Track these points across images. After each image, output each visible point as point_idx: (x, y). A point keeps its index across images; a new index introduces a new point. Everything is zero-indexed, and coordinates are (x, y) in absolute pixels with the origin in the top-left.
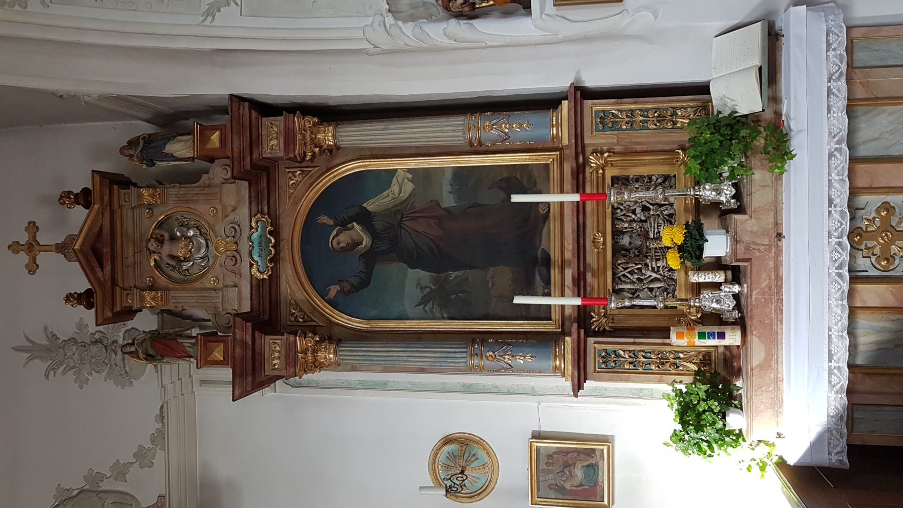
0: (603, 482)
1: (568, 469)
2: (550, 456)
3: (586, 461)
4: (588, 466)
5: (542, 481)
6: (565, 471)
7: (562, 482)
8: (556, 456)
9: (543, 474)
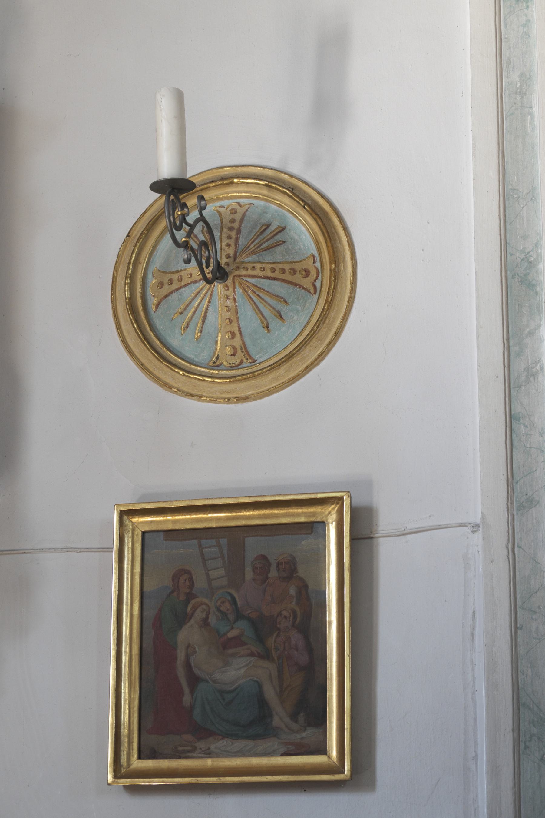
0: (209, 754)
5: (200, 545)
6: (243, 625)
7: (199, 615)
8: (292, 591)
9: (225, 549)
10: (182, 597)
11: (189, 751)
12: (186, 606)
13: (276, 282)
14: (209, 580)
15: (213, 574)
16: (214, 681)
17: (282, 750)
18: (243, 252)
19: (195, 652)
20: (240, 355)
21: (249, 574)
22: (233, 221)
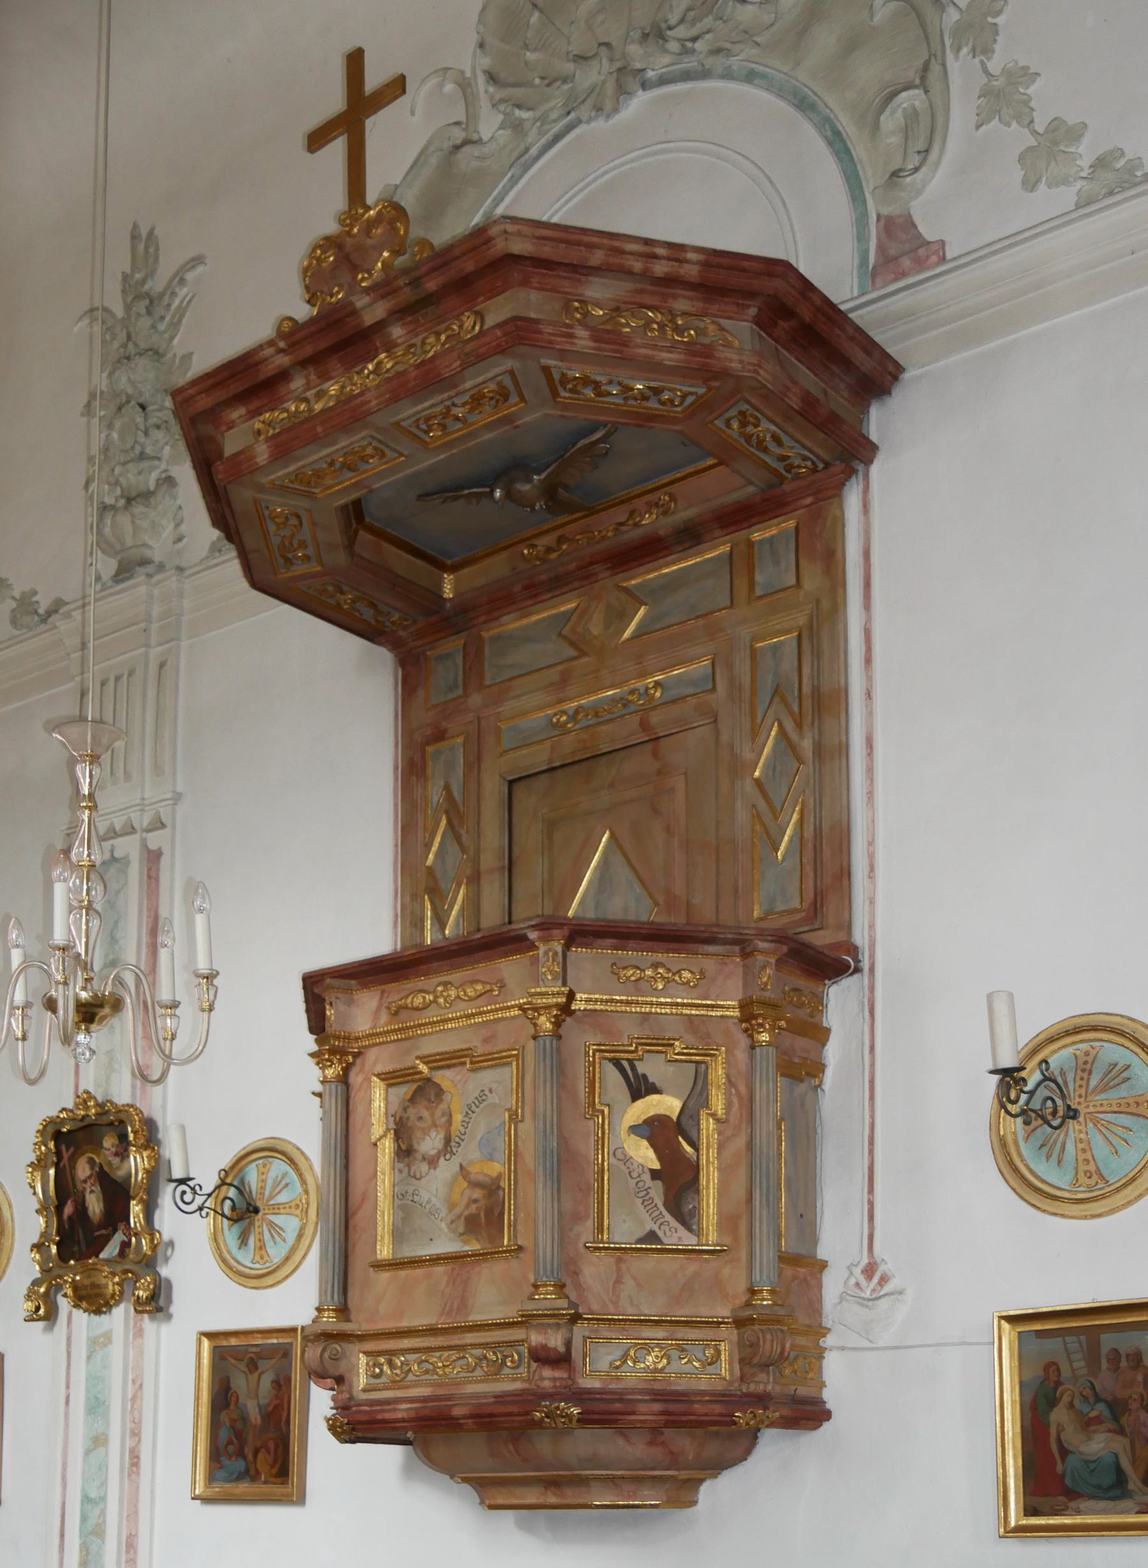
0: (1078, 1512)
1: (1106, 1413)
3: (1134, 1462)
5: (1065, 1343)
6: (1101, 1408)
7: (1066, 1399)
8: (1140, 1378)
9: (1084, 1344)
10: (1052, 1385)
11: (1063, 1510)
12: (1055, 1394)
13: (1122, 1115)
14: (1073, 1370)
15: (1076, 1365)
16: (1080, 1453)
17: (1136, 1509)
18: (1094, 1091)
19: (1064, 1430)
20: (1095, 1177)
21: (1104, 1364)
22: (1086, 1063)
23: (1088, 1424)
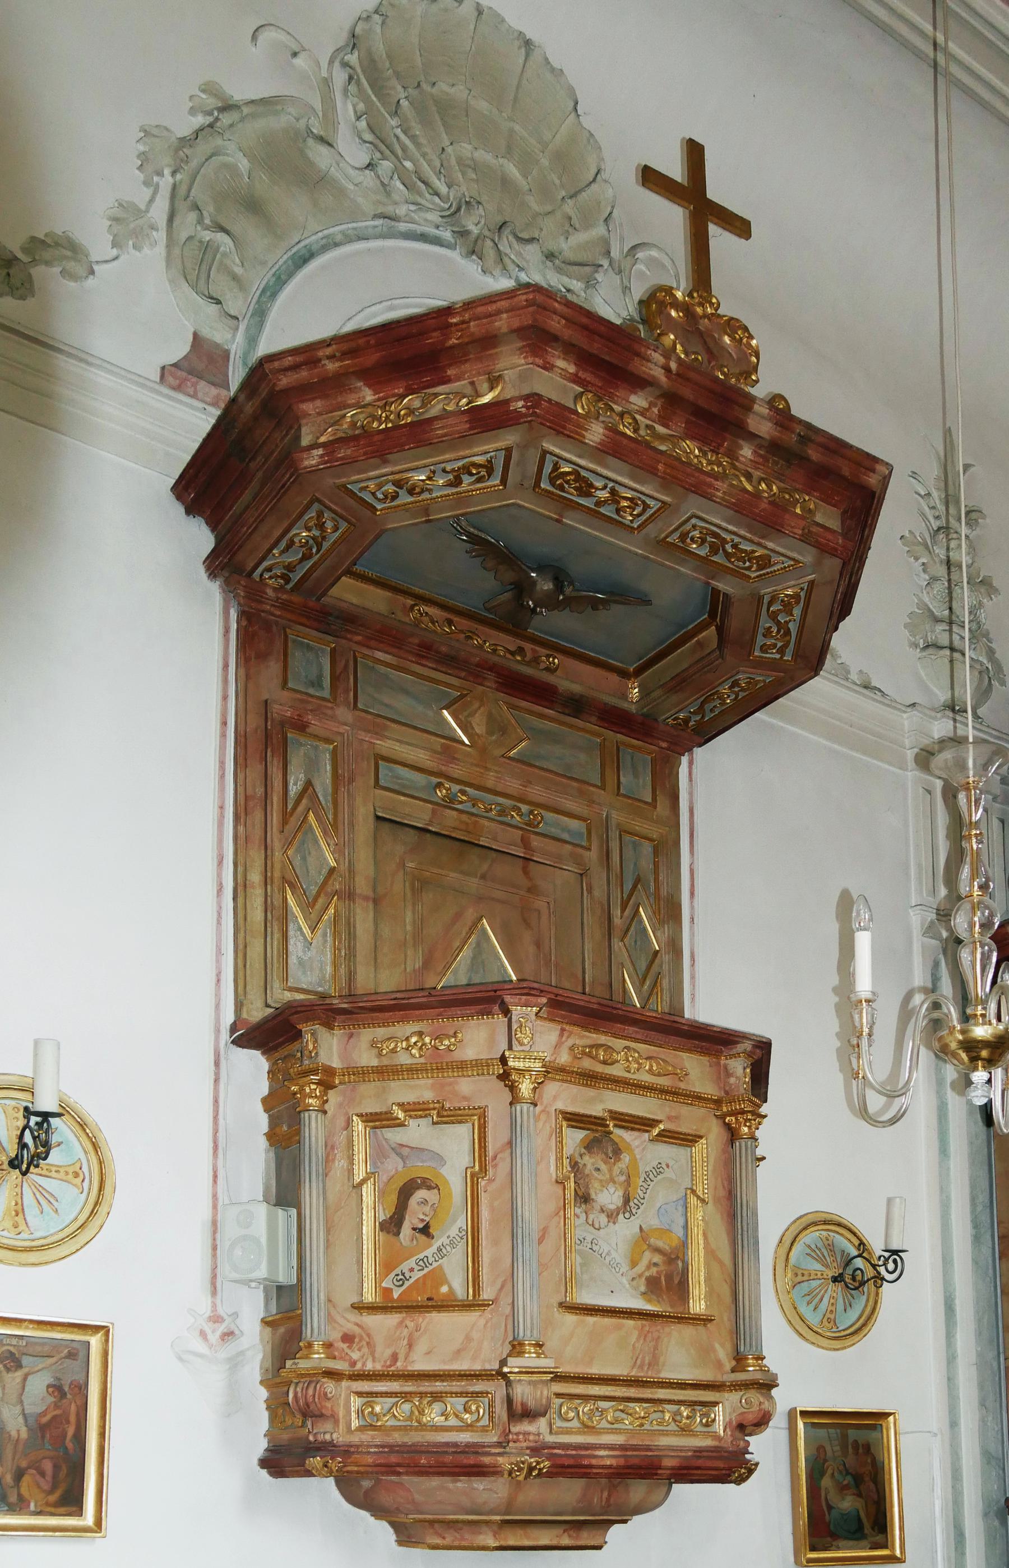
0: (838, 1548)
1: (852, 1482)
2: (867, 1448)
3: (867, 1515)
4: (859, 1520)
8: (869, 1461)
23: (842, 1489)
